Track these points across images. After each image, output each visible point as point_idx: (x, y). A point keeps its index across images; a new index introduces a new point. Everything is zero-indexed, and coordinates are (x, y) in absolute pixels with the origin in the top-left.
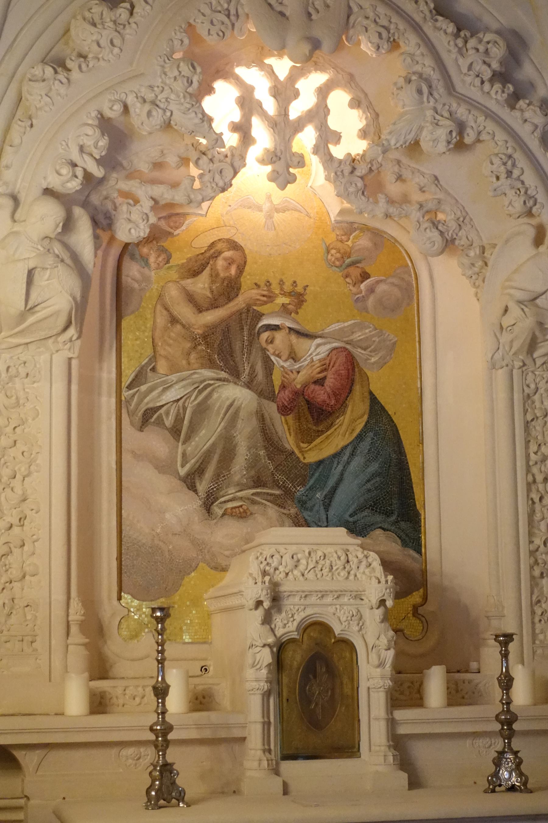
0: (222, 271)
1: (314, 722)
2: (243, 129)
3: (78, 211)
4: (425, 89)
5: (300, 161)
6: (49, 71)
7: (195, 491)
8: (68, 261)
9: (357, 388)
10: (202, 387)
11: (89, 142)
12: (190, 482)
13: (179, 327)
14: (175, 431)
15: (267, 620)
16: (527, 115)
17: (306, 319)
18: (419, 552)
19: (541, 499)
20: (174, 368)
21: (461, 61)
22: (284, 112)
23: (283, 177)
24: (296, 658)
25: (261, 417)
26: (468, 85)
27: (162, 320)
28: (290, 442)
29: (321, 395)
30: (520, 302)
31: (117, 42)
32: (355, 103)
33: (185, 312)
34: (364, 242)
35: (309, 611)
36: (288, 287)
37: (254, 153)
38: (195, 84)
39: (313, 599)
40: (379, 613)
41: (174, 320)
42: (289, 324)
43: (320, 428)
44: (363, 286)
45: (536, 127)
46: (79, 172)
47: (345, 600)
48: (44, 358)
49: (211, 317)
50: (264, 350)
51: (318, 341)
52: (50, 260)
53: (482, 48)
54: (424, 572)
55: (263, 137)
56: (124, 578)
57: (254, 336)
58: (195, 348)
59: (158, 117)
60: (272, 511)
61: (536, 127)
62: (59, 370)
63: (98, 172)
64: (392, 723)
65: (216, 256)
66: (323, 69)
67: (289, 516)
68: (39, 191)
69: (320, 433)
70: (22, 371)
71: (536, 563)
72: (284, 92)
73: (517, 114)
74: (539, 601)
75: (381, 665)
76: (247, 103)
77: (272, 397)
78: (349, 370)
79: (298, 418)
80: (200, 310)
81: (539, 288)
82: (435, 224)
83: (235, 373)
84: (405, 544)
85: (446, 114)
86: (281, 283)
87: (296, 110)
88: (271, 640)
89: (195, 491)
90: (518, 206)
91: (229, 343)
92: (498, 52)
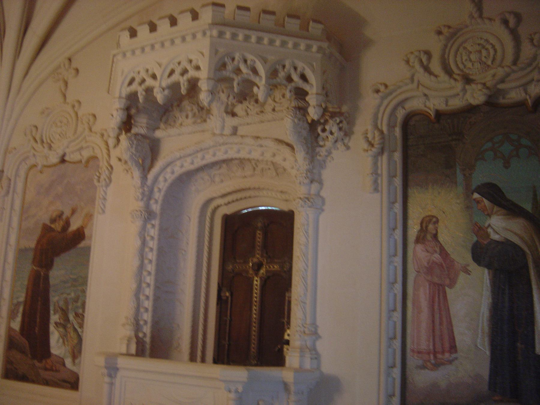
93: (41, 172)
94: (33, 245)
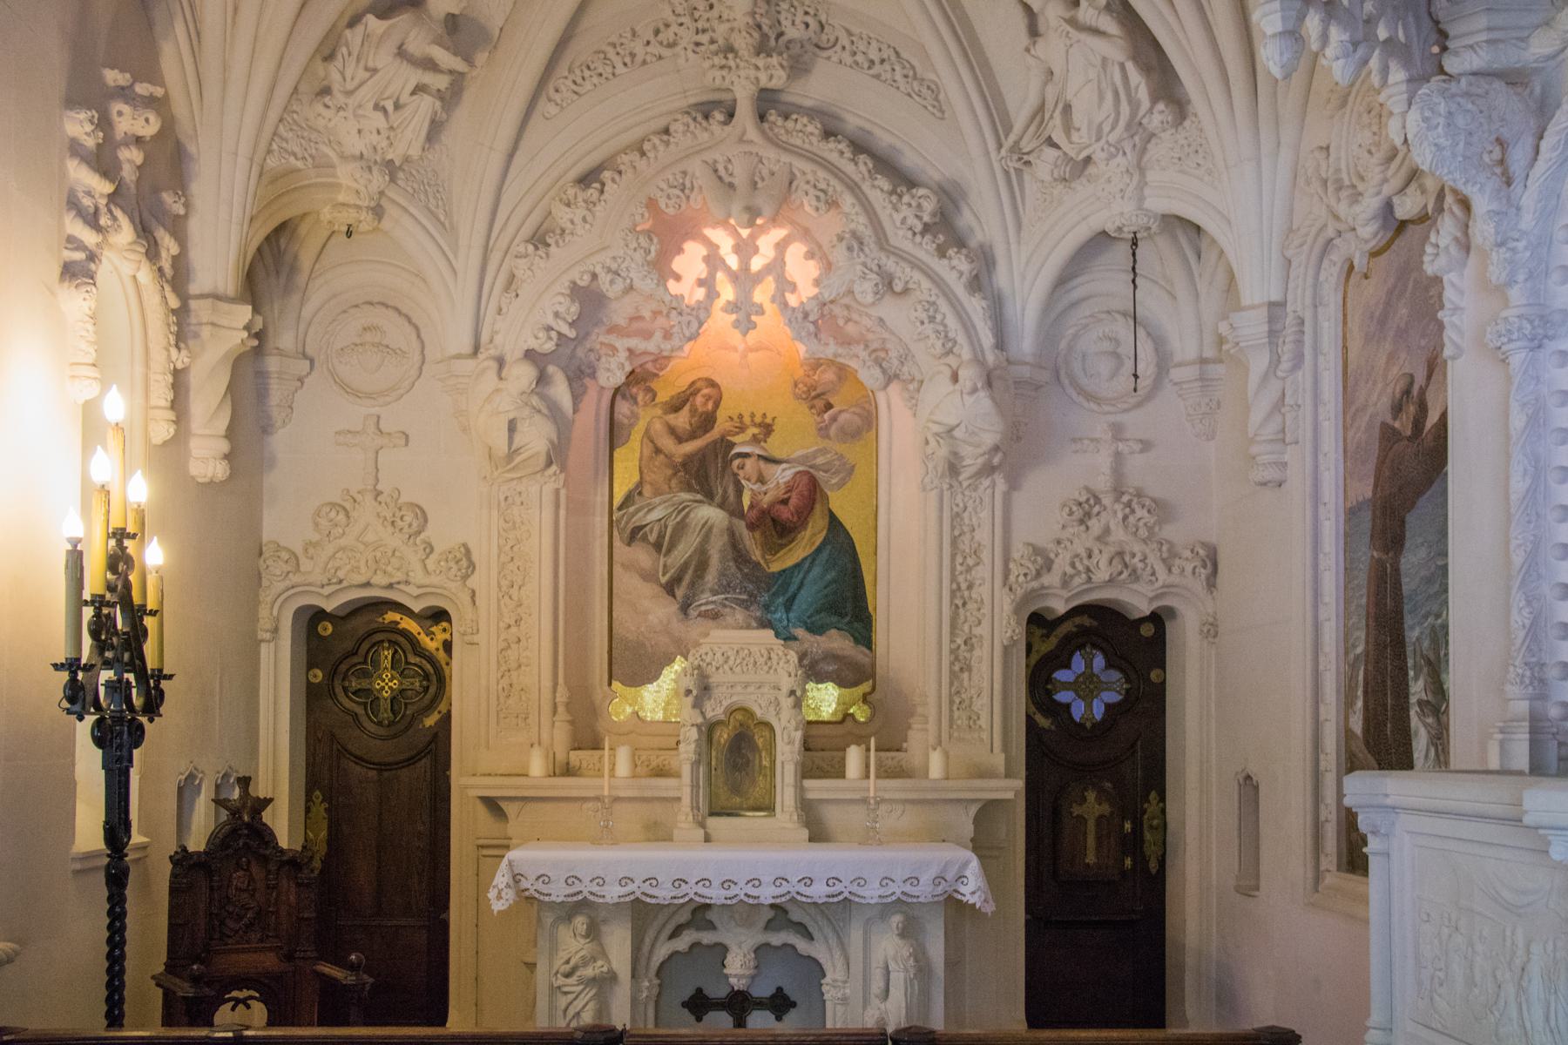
0: (699, 406)
1: (736, 789)
2: (707, 283)
3: (551, 369)
4: (856, 246)
5: (760, 311)
6: (531, 248)
7: (674, 596)
8: (545, 411)
9: (818, 507)
10: (680, 508)
11: (561, 309)
12: (670, 589)
13: (662, 457)
14: (658, 546)
15: (698, 704)
16: (955, 262)
17: (774, 446)
18: (870, 648)
19: (964, 604)
20: (657, 493)
21: (895, 215)
22: (745, 266)
23: (746, 325)
24: (723, 736)
25: (731, 532)
26: (900, 239)
27: (648, 451)
28: (756, 554)
29: (785, 513)
30: (937, 434)
31: (589, 218)
32: (810, 255)
33: (668, 443)
34: (830, 376)
35: (735, 699)
36: (758, 419)
37: (720, 303)
38: (653, 254)
39: (739, 689)
40: (791, 700)
41: (658, 451)
42: (758, 451)
43: (784, 541)
44: (826, 416)
45: (961, 274)
46: (554, 334)
47: (765, 690)
48: (534, 489)
49: (690, 447)
50: (735, 475)
51: (784, 466)
52: (527, 412)
53: (914, 204)
54: (873, 665)
55: (727, 292)
56: (615, 667)
57: (727, 463)
58: (675, 474)
59: (620, 285)
60: (740, 615)
61: (961, 274)
62: (548, 498)
63: (572, 334)
64: (800, 790)
65: (694, 394)
66: (781, 226)
67: (756, 619)
68: (519, 354)
69: (782, 546)
70: (518, 500)
71: (957, 659)
72: (745, 249)
73: (945, 262)
74: (958, 692)
75: (791, 742)
76: (713, 260)
77: (742, 515)
78: (811, 491)
79: (763, 533)
80: (680, 440)
81: (952, 421)
82: (879, 363)
83: (709, 496)
84: (857, 641)
85: (875, 268)
86: (753, 415)
87: (757, 264)
88: (700, 720)
89: (674, 596)
90: (939, 349)
91: (706, 469)
92: (929, 206)
93: (1366, 277)
94: (1369, 494)
